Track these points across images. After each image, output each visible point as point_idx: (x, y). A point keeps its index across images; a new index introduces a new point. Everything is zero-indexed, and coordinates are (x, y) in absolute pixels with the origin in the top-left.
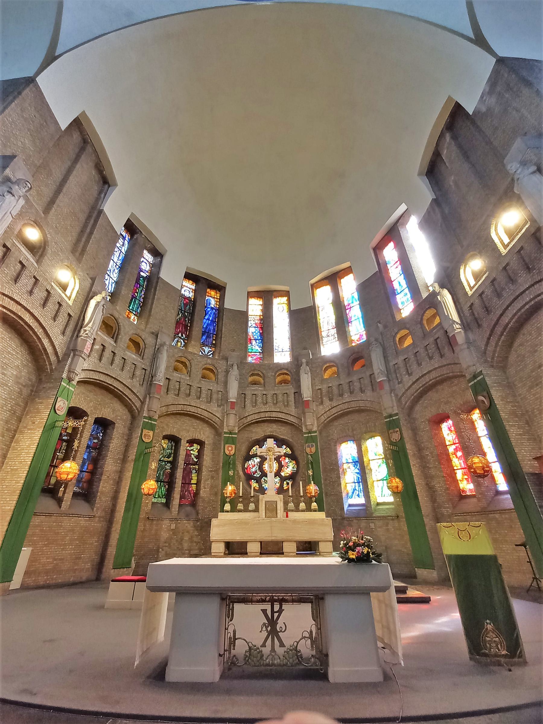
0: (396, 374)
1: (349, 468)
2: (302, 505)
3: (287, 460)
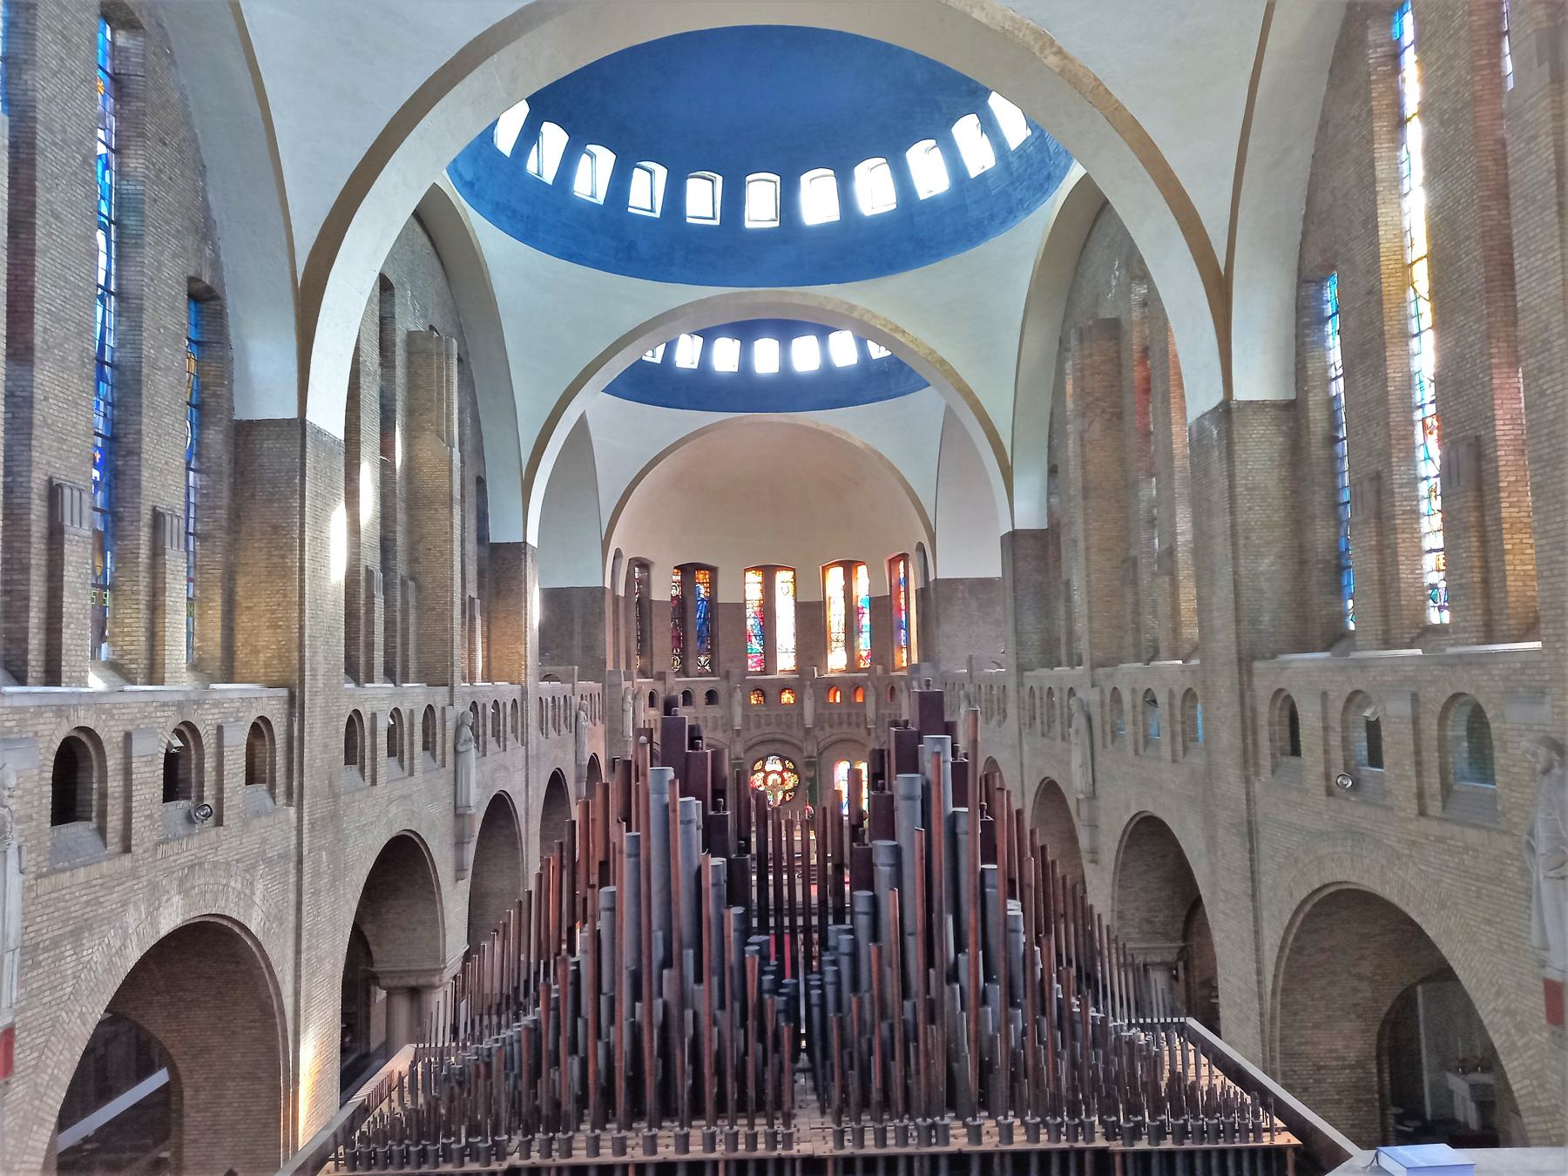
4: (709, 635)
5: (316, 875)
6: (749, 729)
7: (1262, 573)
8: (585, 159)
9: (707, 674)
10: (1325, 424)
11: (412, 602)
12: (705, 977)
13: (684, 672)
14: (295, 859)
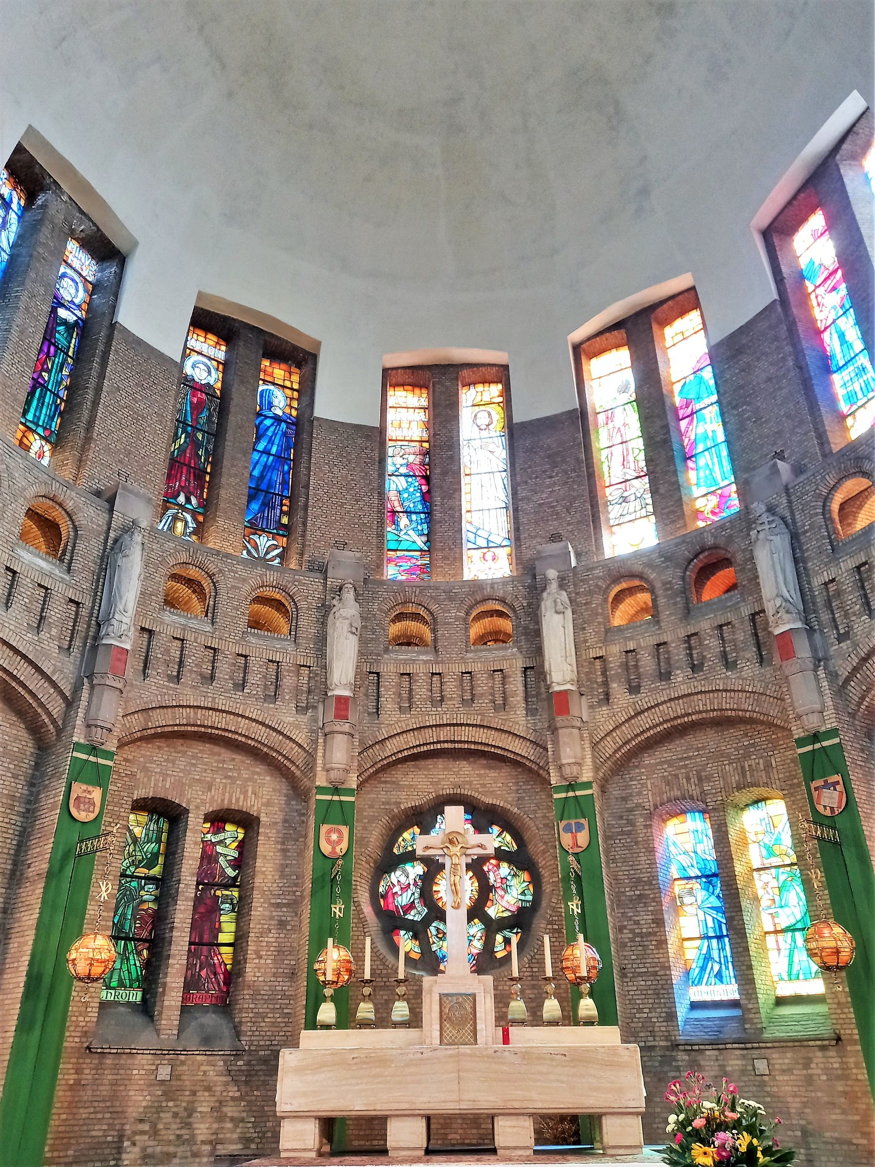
0: (833, 614)
1: (691, 892)
2: (551, 1007)
3: (505, 869)
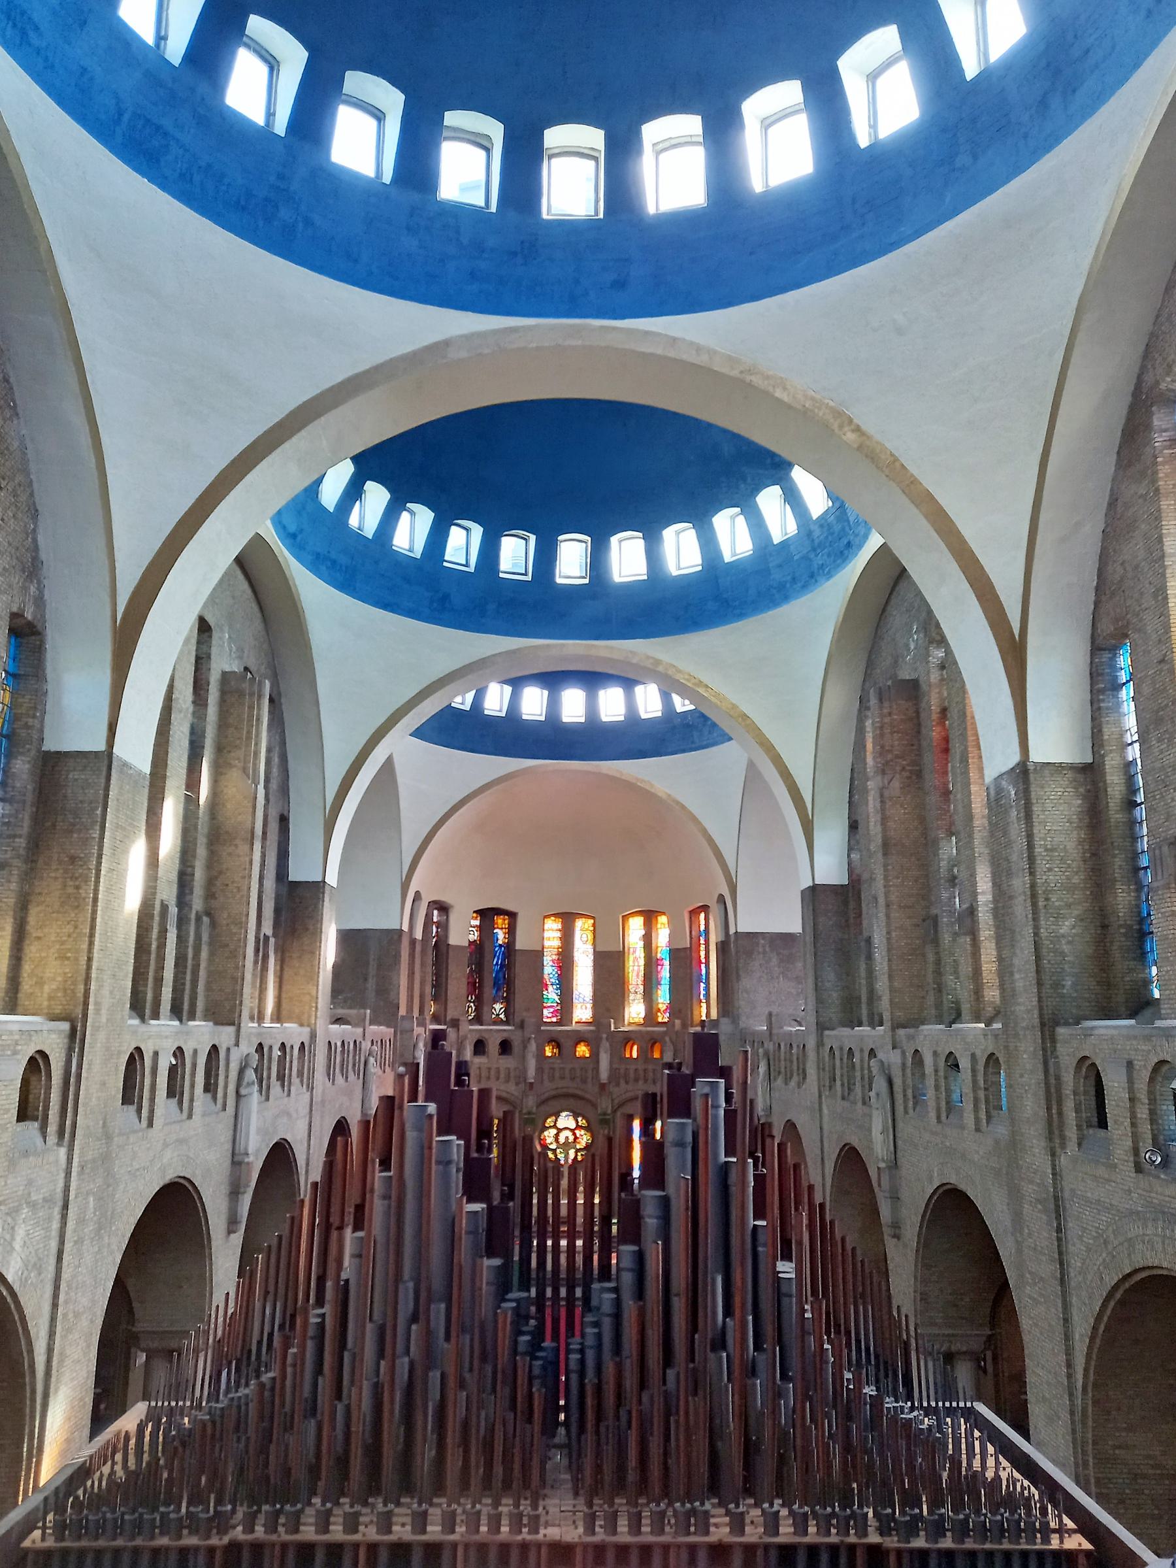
3: (583, 1132)
4: (506, 984)
5: (81, 1221)
6: (542, 1082)
7: (1063, 936)
8: (405, 516)
9: (501, 1022)
10: (1123, 788)
11: (205, 937)
12: (453, 1334)
13: (478, 1019)
14: (60, 1203)
